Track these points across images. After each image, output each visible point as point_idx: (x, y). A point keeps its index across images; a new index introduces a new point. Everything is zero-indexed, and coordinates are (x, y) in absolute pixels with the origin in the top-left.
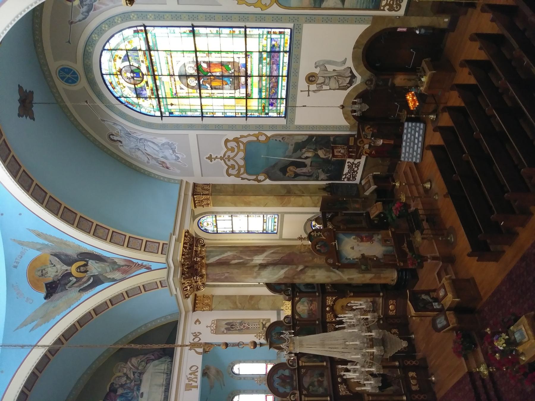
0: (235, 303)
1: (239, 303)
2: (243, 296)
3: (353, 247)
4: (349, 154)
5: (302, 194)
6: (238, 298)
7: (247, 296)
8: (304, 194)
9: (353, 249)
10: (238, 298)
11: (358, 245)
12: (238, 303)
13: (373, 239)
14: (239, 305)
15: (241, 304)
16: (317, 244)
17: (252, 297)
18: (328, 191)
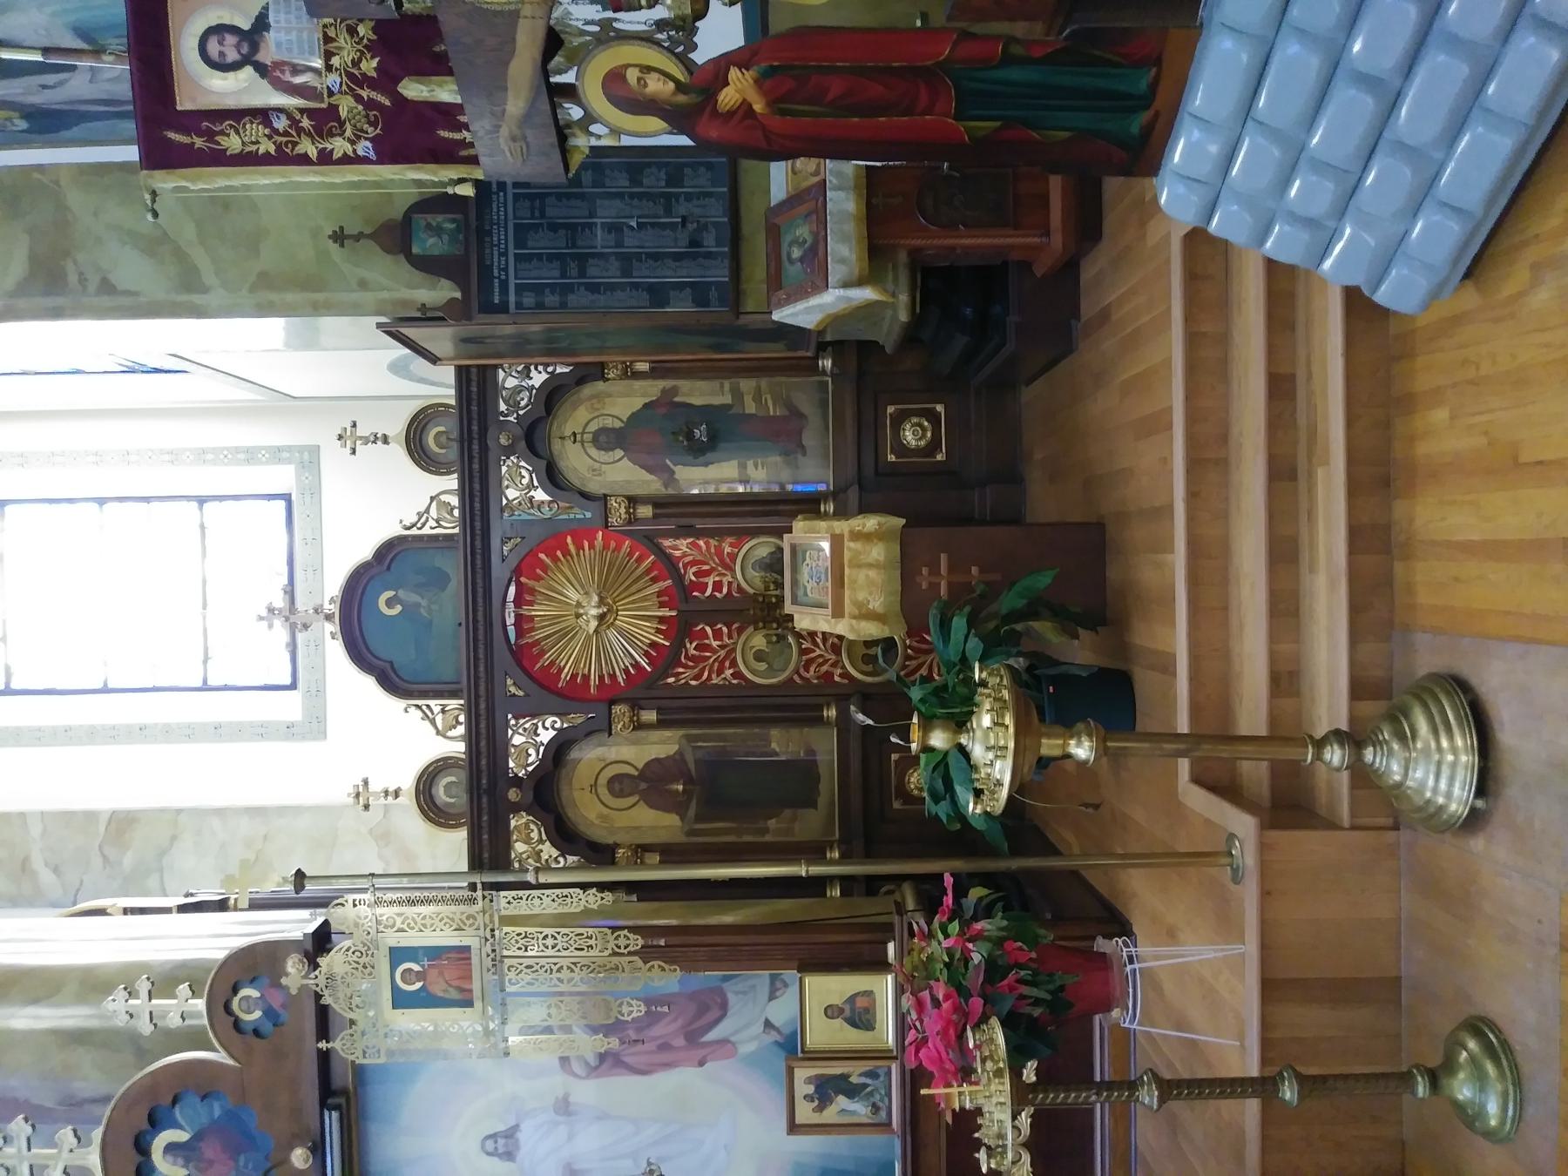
0: (25, 865)
1: (46, 865)
2: (67, 817)
3: (511, 1134)
4: (387, 80)
5: (184, 298)
6: (36, 830)
7: (90, 816)
8: (197, 299)
9: (509, 1156)
10: (36, 830)
11: (564, 1107)
12: (37, 863)
13: (712, 1035)
14: (46, 877)
15: (56, 870)
16: (156, 1122)
17: (122, 824)
18: (428, 266)
